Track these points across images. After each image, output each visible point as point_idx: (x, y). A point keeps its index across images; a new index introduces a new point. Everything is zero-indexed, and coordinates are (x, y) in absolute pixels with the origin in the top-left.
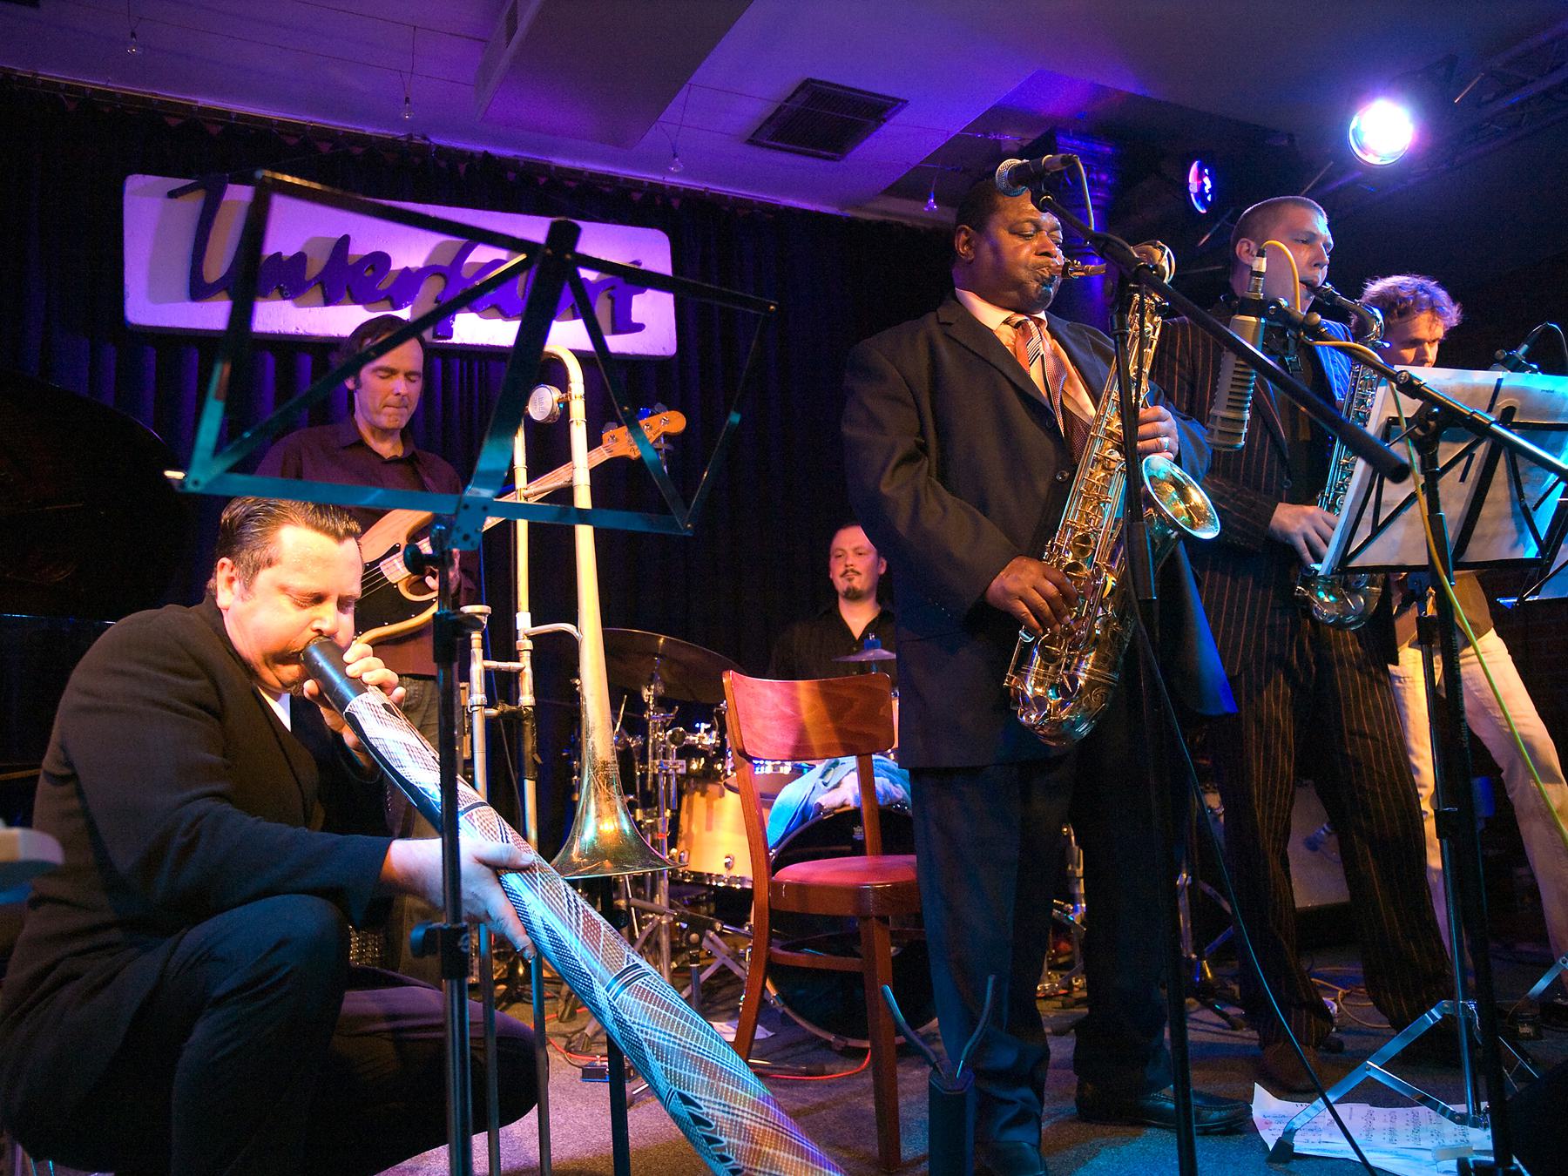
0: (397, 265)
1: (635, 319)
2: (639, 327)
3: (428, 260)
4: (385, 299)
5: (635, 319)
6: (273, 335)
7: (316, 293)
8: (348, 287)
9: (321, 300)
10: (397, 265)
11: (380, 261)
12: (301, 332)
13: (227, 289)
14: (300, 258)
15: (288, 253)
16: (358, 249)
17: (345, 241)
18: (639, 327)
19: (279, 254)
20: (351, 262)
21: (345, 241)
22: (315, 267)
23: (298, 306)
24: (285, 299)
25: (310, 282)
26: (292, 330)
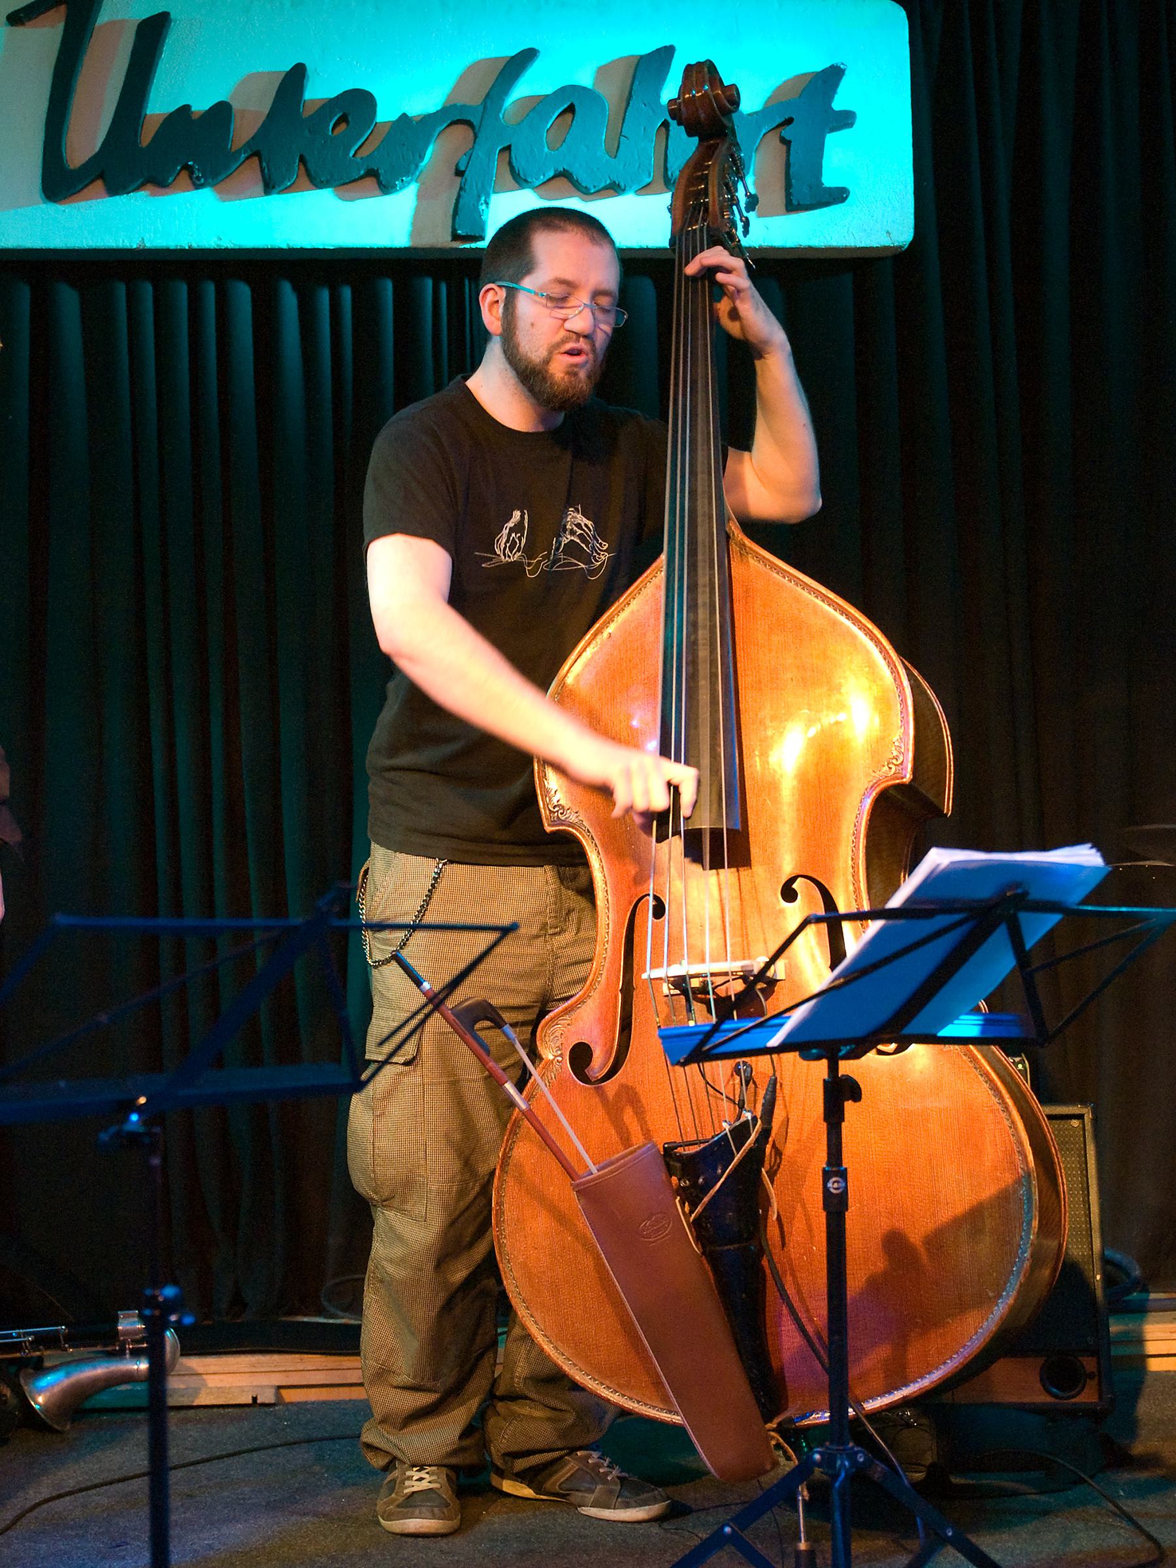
0: (386, 113)
1: (829, 180)
2: (839, 196)
3: (449, 97)
4: (372, 173)
5: (829, 180)
6: (182, 251)
7: (251, 173)
8: (302, 160)
9: (260, 187)
10: (386, 113)
12: (226, 243)
13: (101, 176)
14: (222, 111)
15: (201, 104)
17: (297, 75)
18: (839, 196)
19: (186, 109)
20: (306, 113)
21: (297, 75)
25: (239, 152)
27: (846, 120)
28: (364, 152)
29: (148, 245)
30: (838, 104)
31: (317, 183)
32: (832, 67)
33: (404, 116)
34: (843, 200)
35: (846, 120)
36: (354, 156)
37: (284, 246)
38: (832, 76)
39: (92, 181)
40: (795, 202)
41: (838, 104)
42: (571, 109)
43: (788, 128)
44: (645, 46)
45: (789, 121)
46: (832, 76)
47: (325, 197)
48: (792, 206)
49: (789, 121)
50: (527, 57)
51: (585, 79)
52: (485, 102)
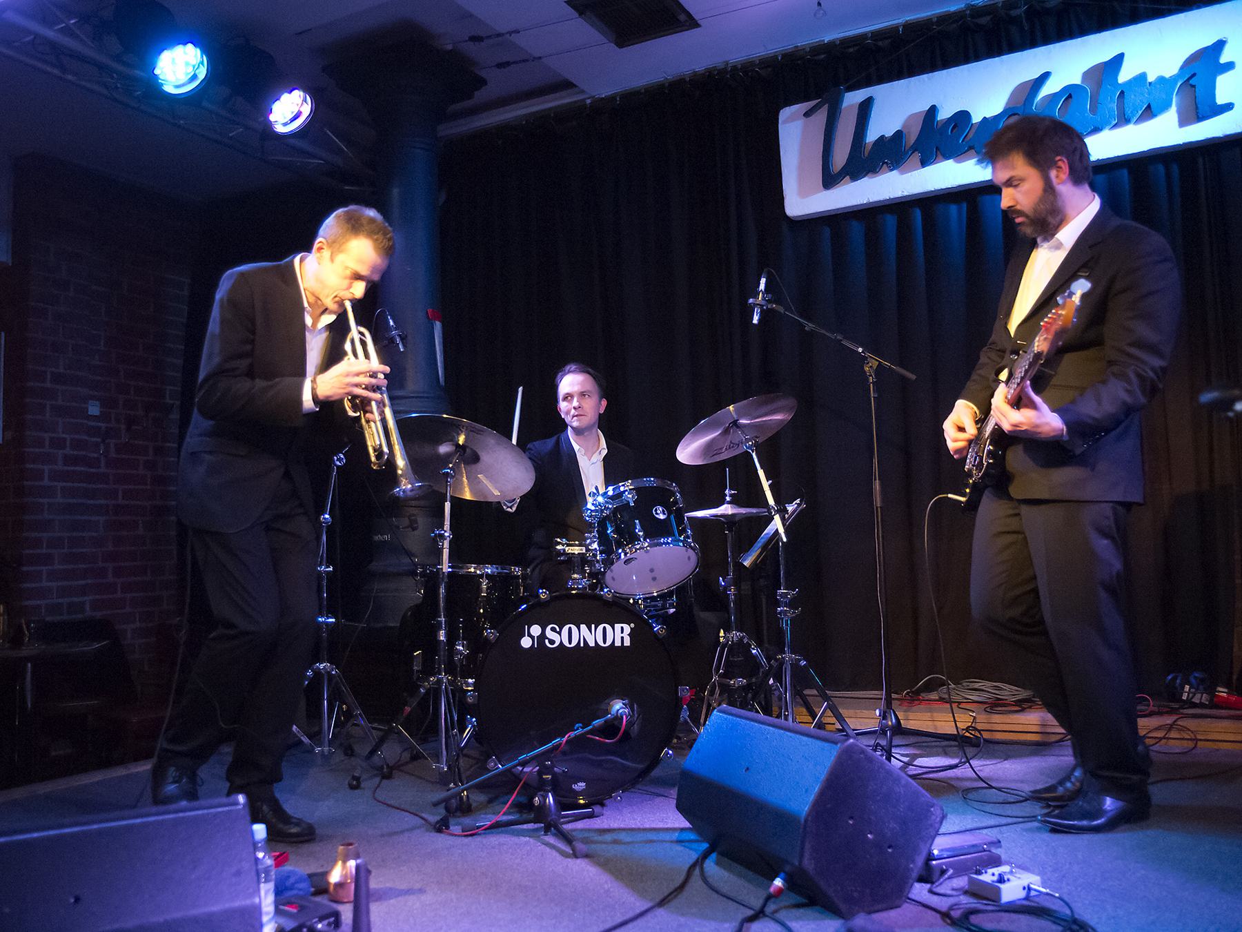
0: (976, 119)
1: (1220, 100)
2: (1229, 107)
3: (1007, 104)
4: (971, 148)
5: (1220, 100)
10: (976, 119)
11: (963, 116)
12: (906, 194)
14: (899, 134)
15: (889, 133)
16: (944, 114)
17: (933, 110)
18: (1229, 107)
19: (883, 137)
21: (933, 110)
22: (912, 137)
23: (902, 173)
24: (892, 170)
26: (899, 194)
27: (1230, 66)
28: (967, 139)
29: (871, 201)
30: (1223, 59)
31: (947, 158)
32: (1218, 41)
33: (985, 117)
34: (1232, 109)
35: (1230, 66)
36: (962, 141)
37: (933, 189)
38: (1220, 45)
39: (844, 177)
40: (1200, 116)
41: (1223, 59)
42: (1070, 96)
43: (1193, 79)
44: (1106, 56)
45: (1194, 75)
46: (1220, 45)
47: (950, 164)
48: (1200, 117)
49: (1194, 75)
50: (1045, 76)
51: (1077, 80)
52: (1024, 104)
